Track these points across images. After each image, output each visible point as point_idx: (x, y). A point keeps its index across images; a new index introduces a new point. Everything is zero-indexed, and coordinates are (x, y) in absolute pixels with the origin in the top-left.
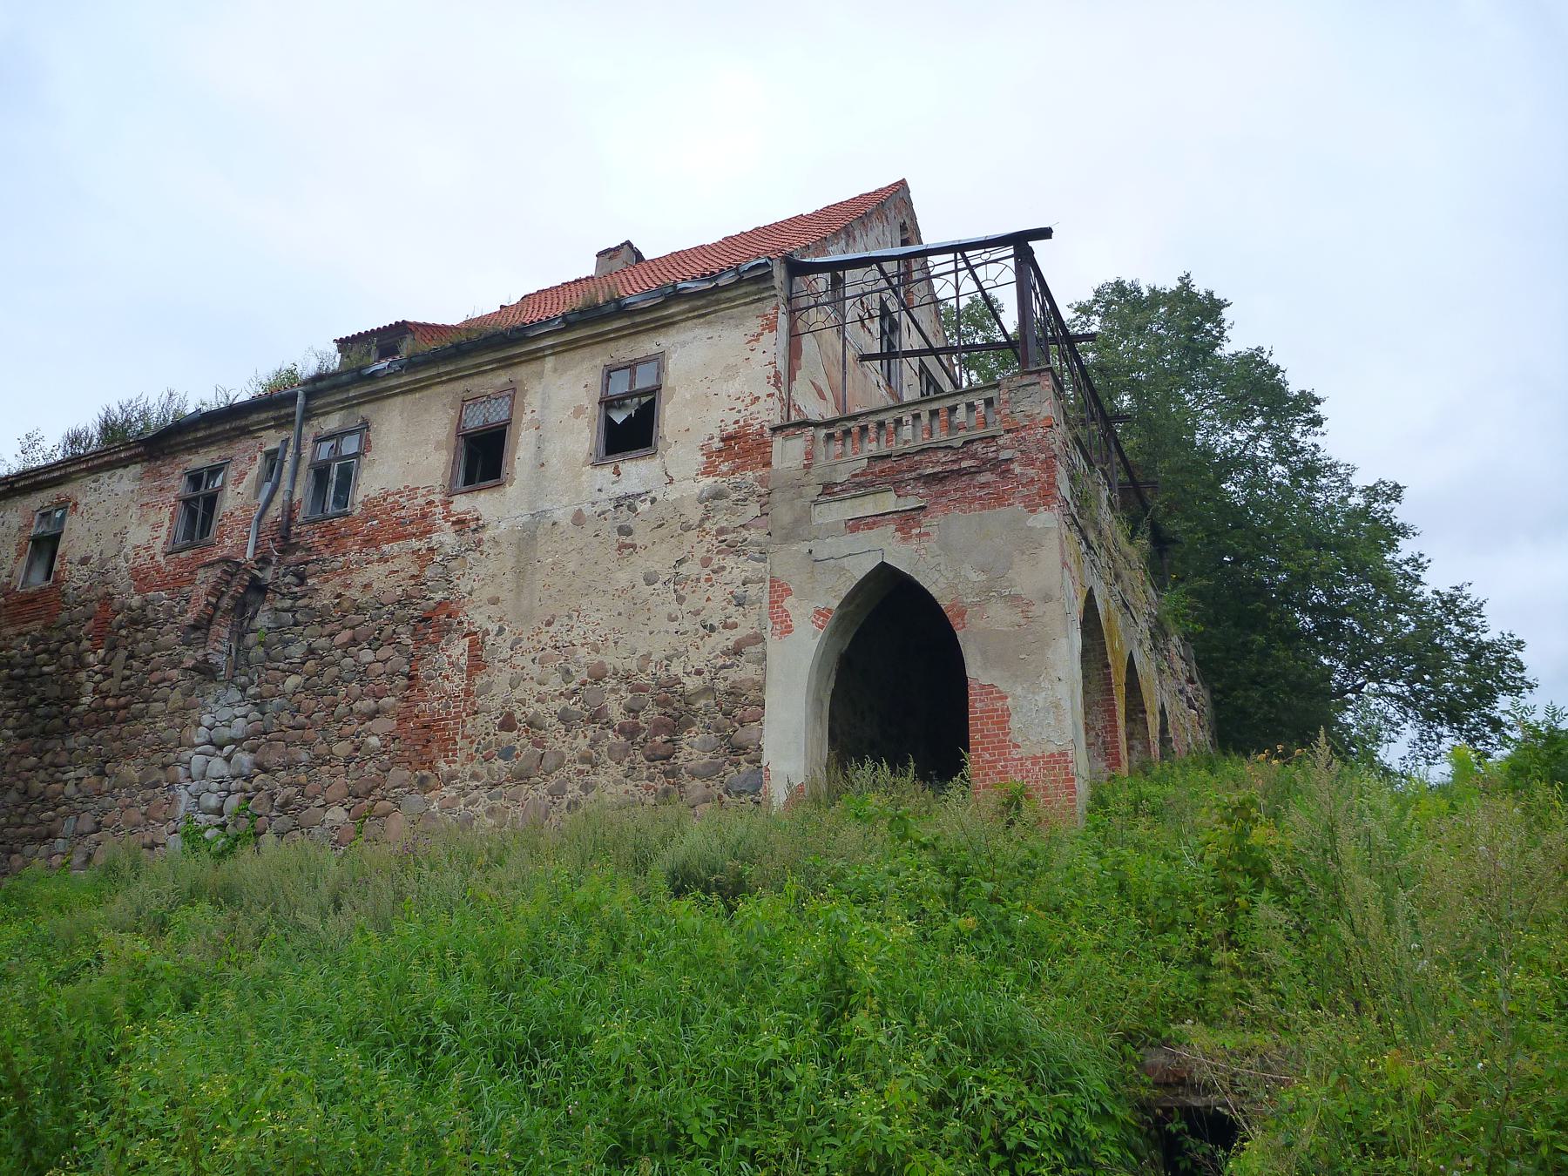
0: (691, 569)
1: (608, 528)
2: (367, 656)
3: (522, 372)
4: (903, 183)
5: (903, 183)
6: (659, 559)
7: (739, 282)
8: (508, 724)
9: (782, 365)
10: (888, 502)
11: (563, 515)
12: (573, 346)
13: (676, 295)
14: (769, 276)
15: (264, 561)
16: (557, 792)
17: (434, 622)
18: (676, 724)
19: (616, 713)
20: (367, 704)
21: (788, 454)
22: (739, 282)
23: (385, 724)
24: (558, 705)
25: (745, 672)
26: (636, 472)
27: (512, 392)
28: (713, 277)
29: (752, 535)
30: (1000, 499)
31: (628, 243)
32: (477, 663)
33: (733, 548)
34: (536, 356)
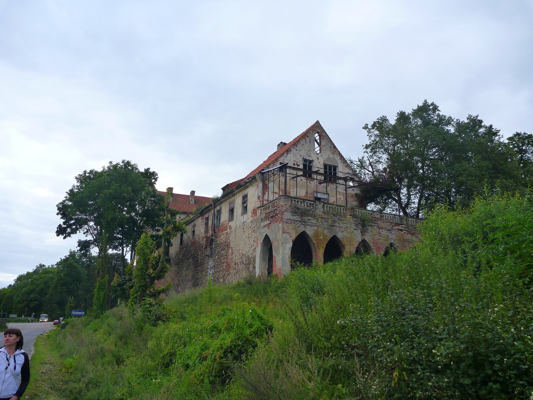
0: (250, 235)
1: (242, 228)
2: (223, 252)
3: (235, 196)
4: (318, 122)
5: (318, 122)
6: (246, 234)
7: (252, 180)
8: (235, 264)
9: (260, 194)
10: (268, 222)
11: (238, 226)
12: (239, 192)
13: (246, 183)
14: (255, 178)
15: (212, 235)
16: (240, 276)
17: (228, 246)
18: (249, 264)
19: (244, 261)
20: (223, 261)
21: (259, 212)
22: (252, 180)
23: (225, 264)
24: (240, 260)
25: (254, 255)
26: (245, 216)
27: (234, 201)
28: (249, 179)
29: (255, 229)
30: (277, 221)
31: (282, 142)
32: (232, 254)
33: (254, 231)
34: (236, 194)
